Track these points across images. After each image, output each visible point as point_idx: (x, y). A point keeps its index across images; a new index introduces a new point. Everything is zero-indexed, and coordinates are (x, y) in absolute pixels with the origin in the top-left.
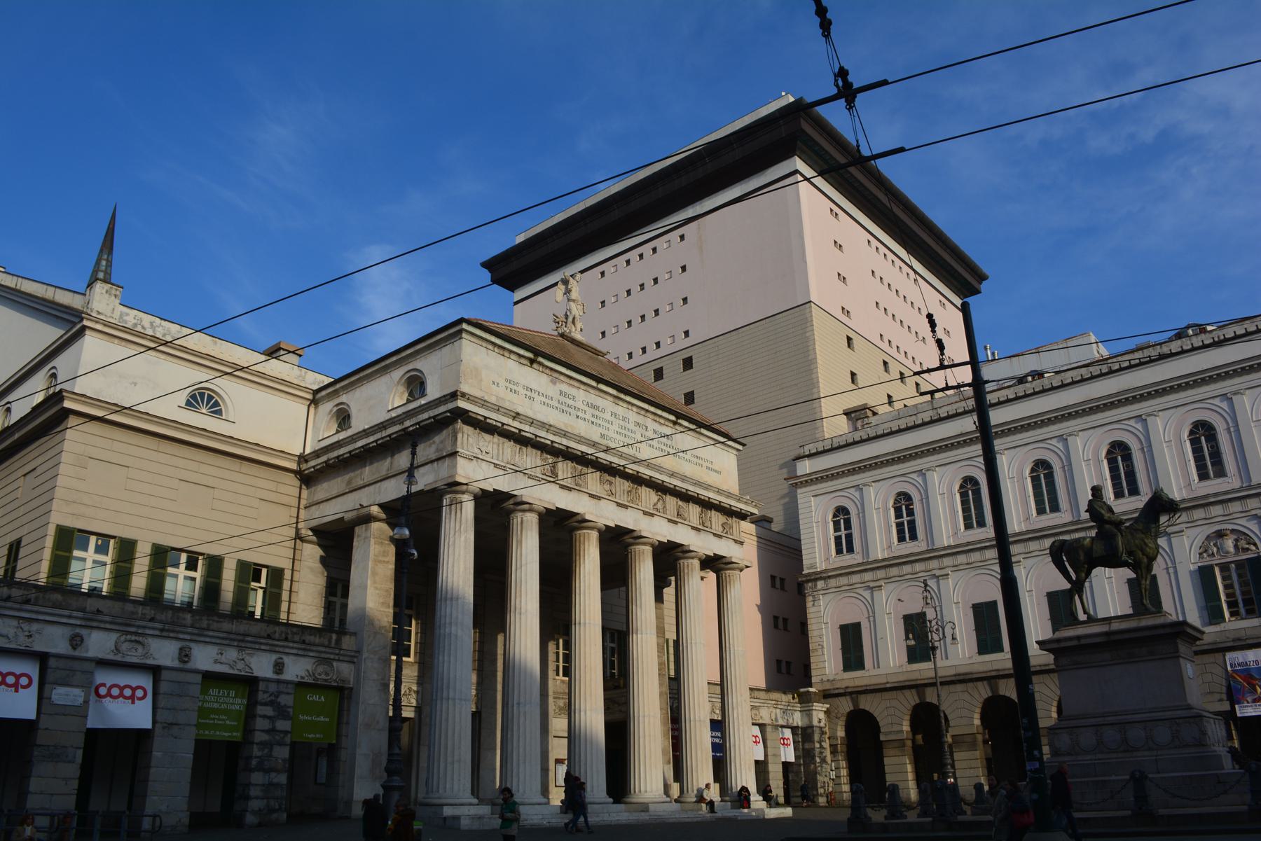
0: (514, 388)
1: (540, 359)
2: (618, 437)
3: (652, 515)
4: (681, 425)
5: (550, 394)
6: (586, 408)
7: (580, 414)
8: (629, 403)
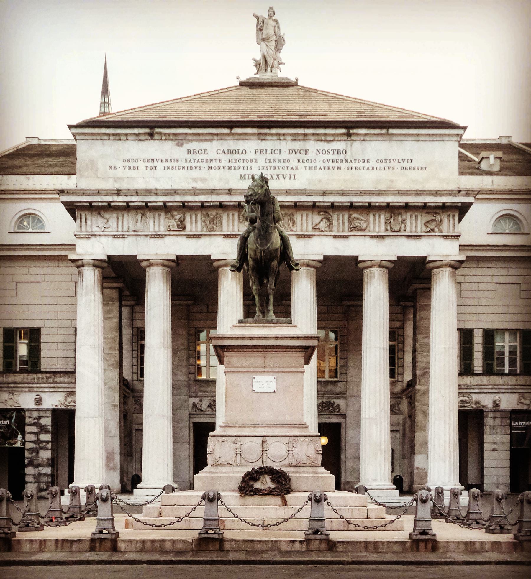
0: (132, 165)
1: (158, 130)
3: (310, 236)
4: (358, 135)
5: (175, 156)
6: (222, 156)
7: (213, 164)
8: (279, 135)
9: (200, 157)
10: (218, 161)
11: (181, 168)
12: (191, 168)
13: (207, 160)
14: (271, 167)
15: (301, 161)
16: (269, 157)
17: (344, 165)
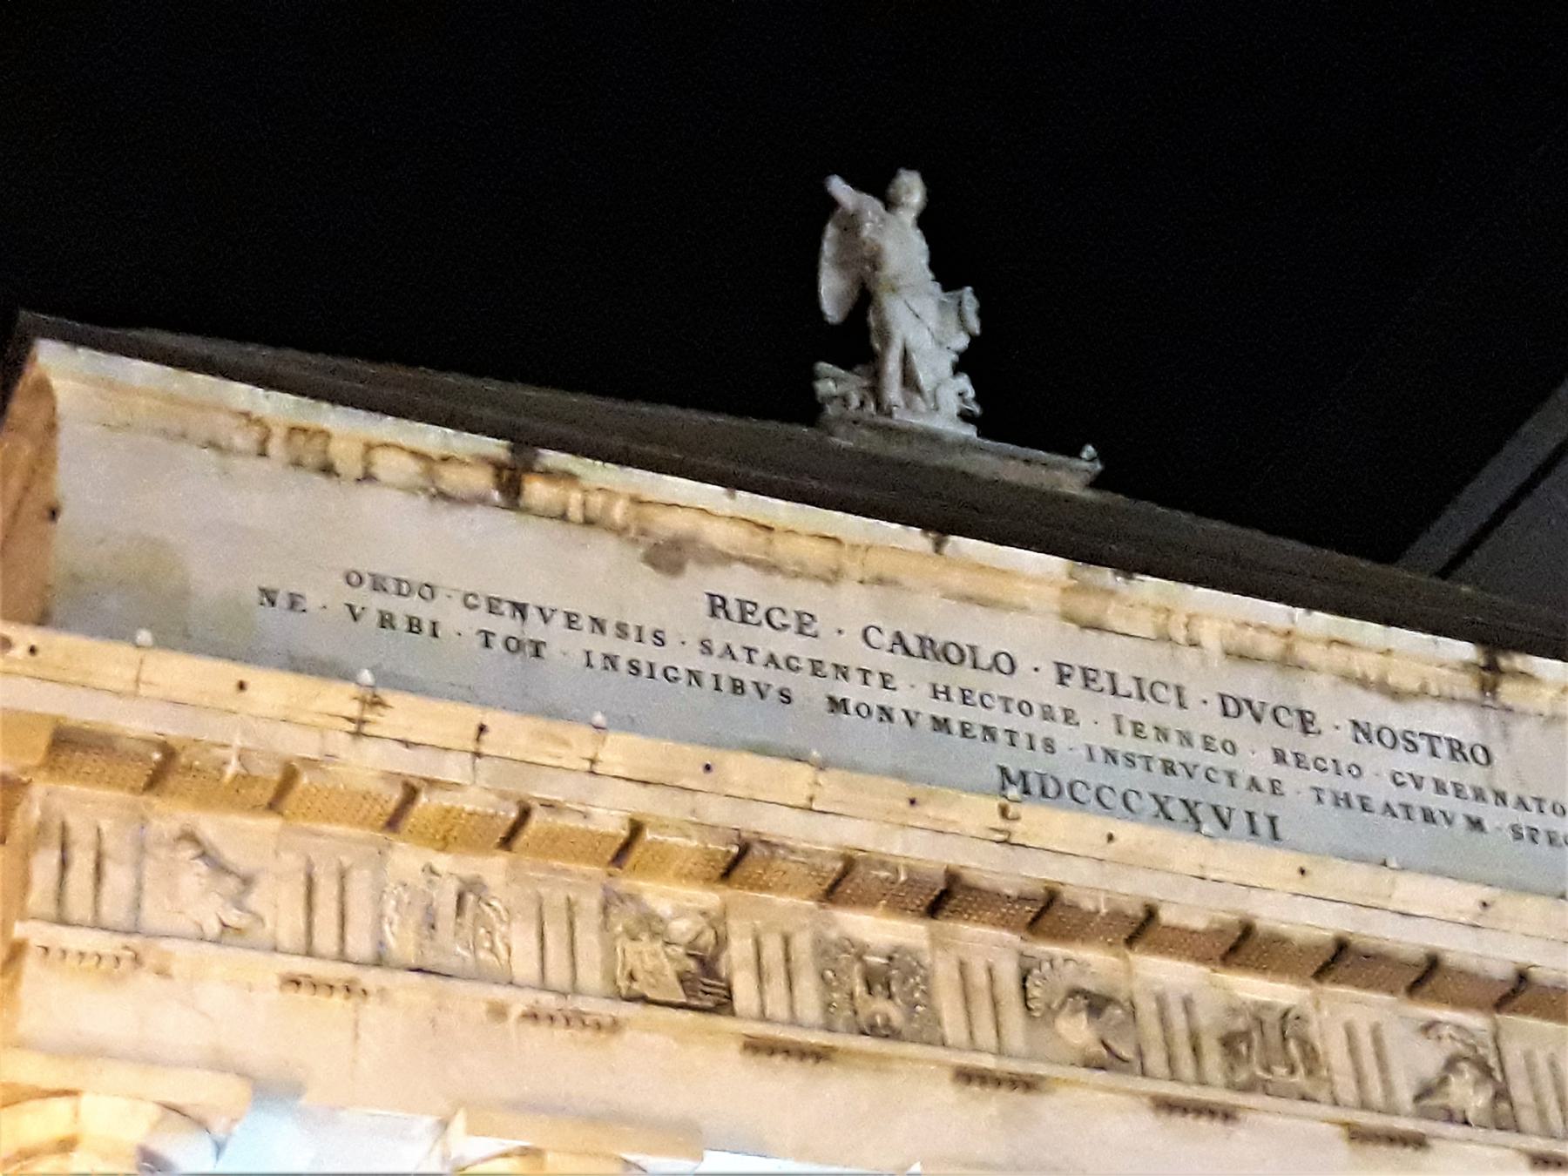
2: (1122, 777)
7: (851, 691)
9: (786, 644)
10: (875, 680)
11: (683, 675)
12: (738, 687)
13: (816, 667)
14: (1148, 758)
15: (1290, 758)
16: (1133, 710)
17: (1490, 813)
